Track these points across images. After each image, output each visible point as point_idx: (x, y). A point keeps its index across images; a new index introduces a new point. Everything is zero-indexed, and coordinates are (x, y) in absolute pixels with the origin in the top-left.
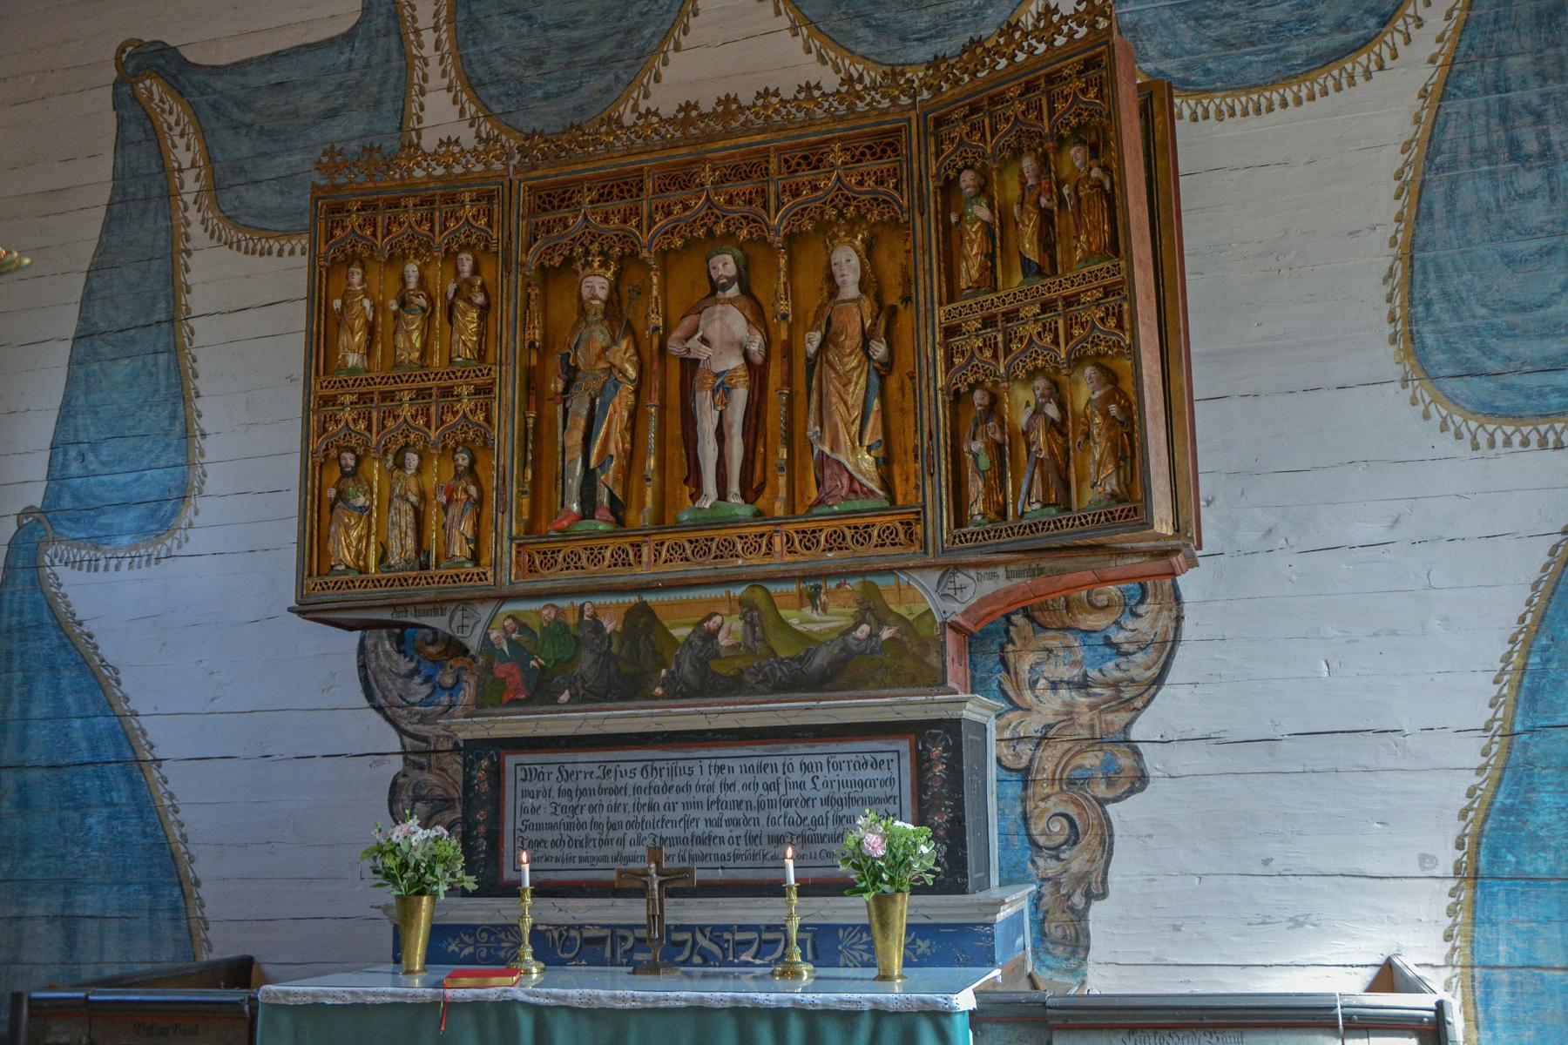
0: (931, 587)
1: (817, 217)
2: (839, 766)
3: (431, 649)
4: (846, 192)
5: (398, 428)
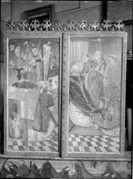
0: (125, 166)
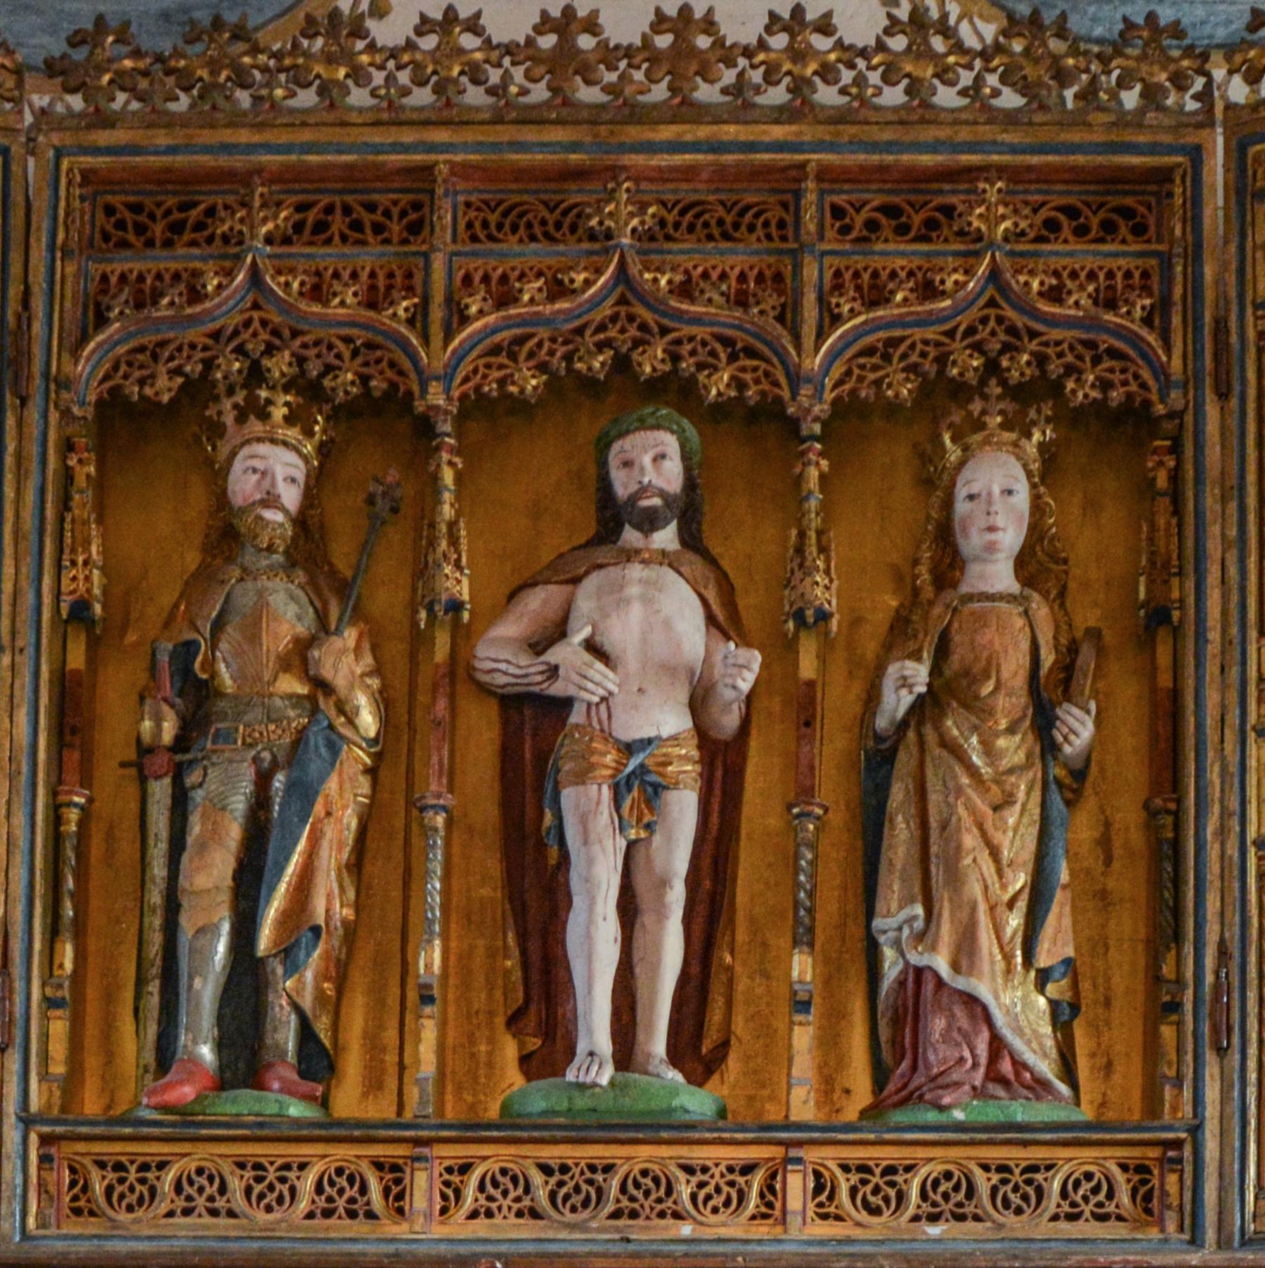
4: (1010, 313)
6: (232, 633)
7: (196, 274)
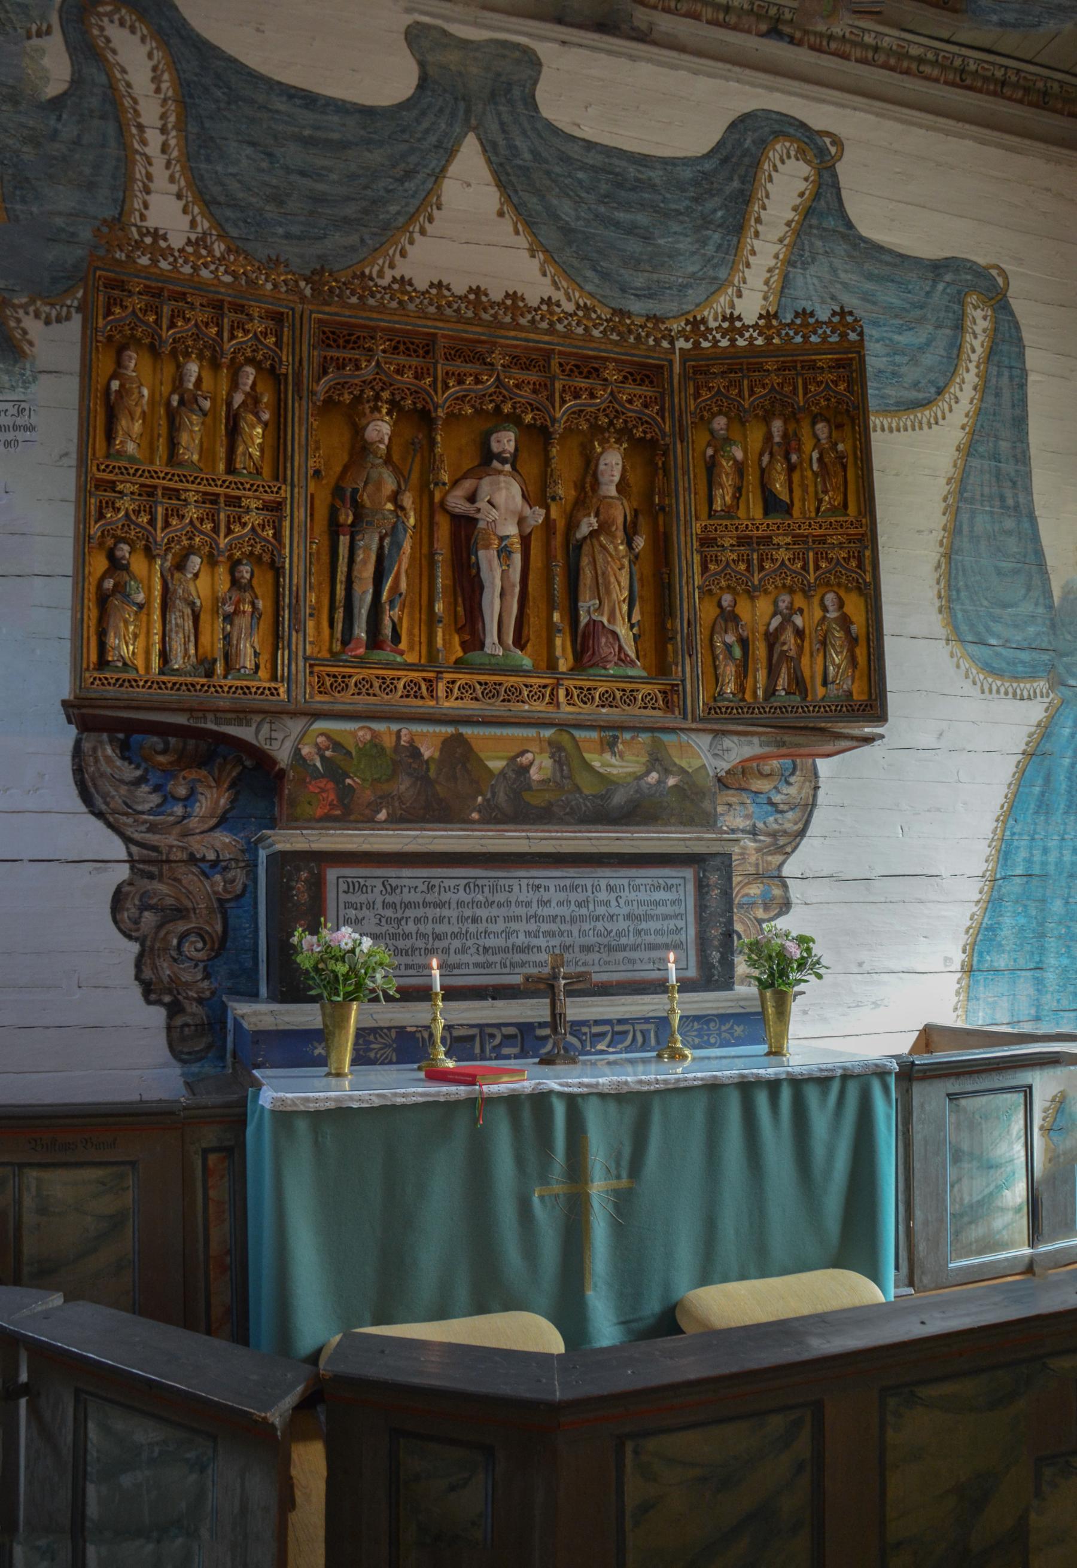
0: (705, 747)
1: (592, 420)
2: (638, 888)
3: (161, 759)
4: (616, 406)
5: (183, 528)
6: (370, 488)
7: (356, 360)
